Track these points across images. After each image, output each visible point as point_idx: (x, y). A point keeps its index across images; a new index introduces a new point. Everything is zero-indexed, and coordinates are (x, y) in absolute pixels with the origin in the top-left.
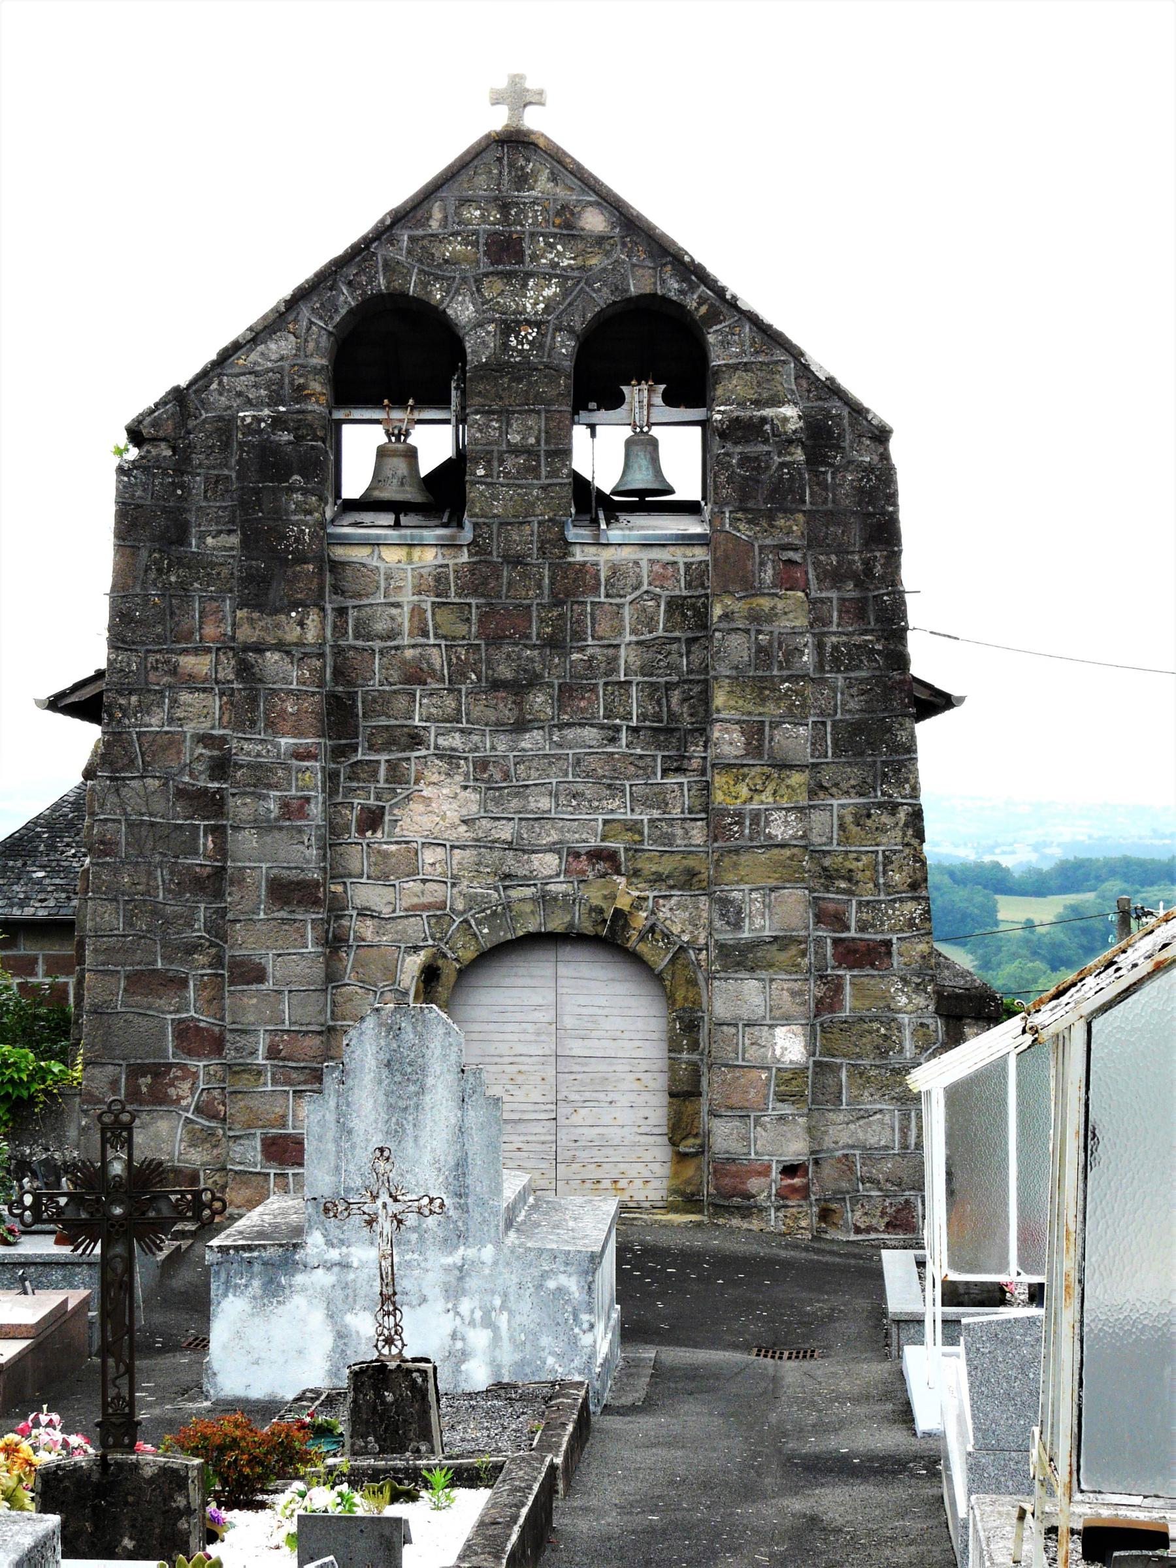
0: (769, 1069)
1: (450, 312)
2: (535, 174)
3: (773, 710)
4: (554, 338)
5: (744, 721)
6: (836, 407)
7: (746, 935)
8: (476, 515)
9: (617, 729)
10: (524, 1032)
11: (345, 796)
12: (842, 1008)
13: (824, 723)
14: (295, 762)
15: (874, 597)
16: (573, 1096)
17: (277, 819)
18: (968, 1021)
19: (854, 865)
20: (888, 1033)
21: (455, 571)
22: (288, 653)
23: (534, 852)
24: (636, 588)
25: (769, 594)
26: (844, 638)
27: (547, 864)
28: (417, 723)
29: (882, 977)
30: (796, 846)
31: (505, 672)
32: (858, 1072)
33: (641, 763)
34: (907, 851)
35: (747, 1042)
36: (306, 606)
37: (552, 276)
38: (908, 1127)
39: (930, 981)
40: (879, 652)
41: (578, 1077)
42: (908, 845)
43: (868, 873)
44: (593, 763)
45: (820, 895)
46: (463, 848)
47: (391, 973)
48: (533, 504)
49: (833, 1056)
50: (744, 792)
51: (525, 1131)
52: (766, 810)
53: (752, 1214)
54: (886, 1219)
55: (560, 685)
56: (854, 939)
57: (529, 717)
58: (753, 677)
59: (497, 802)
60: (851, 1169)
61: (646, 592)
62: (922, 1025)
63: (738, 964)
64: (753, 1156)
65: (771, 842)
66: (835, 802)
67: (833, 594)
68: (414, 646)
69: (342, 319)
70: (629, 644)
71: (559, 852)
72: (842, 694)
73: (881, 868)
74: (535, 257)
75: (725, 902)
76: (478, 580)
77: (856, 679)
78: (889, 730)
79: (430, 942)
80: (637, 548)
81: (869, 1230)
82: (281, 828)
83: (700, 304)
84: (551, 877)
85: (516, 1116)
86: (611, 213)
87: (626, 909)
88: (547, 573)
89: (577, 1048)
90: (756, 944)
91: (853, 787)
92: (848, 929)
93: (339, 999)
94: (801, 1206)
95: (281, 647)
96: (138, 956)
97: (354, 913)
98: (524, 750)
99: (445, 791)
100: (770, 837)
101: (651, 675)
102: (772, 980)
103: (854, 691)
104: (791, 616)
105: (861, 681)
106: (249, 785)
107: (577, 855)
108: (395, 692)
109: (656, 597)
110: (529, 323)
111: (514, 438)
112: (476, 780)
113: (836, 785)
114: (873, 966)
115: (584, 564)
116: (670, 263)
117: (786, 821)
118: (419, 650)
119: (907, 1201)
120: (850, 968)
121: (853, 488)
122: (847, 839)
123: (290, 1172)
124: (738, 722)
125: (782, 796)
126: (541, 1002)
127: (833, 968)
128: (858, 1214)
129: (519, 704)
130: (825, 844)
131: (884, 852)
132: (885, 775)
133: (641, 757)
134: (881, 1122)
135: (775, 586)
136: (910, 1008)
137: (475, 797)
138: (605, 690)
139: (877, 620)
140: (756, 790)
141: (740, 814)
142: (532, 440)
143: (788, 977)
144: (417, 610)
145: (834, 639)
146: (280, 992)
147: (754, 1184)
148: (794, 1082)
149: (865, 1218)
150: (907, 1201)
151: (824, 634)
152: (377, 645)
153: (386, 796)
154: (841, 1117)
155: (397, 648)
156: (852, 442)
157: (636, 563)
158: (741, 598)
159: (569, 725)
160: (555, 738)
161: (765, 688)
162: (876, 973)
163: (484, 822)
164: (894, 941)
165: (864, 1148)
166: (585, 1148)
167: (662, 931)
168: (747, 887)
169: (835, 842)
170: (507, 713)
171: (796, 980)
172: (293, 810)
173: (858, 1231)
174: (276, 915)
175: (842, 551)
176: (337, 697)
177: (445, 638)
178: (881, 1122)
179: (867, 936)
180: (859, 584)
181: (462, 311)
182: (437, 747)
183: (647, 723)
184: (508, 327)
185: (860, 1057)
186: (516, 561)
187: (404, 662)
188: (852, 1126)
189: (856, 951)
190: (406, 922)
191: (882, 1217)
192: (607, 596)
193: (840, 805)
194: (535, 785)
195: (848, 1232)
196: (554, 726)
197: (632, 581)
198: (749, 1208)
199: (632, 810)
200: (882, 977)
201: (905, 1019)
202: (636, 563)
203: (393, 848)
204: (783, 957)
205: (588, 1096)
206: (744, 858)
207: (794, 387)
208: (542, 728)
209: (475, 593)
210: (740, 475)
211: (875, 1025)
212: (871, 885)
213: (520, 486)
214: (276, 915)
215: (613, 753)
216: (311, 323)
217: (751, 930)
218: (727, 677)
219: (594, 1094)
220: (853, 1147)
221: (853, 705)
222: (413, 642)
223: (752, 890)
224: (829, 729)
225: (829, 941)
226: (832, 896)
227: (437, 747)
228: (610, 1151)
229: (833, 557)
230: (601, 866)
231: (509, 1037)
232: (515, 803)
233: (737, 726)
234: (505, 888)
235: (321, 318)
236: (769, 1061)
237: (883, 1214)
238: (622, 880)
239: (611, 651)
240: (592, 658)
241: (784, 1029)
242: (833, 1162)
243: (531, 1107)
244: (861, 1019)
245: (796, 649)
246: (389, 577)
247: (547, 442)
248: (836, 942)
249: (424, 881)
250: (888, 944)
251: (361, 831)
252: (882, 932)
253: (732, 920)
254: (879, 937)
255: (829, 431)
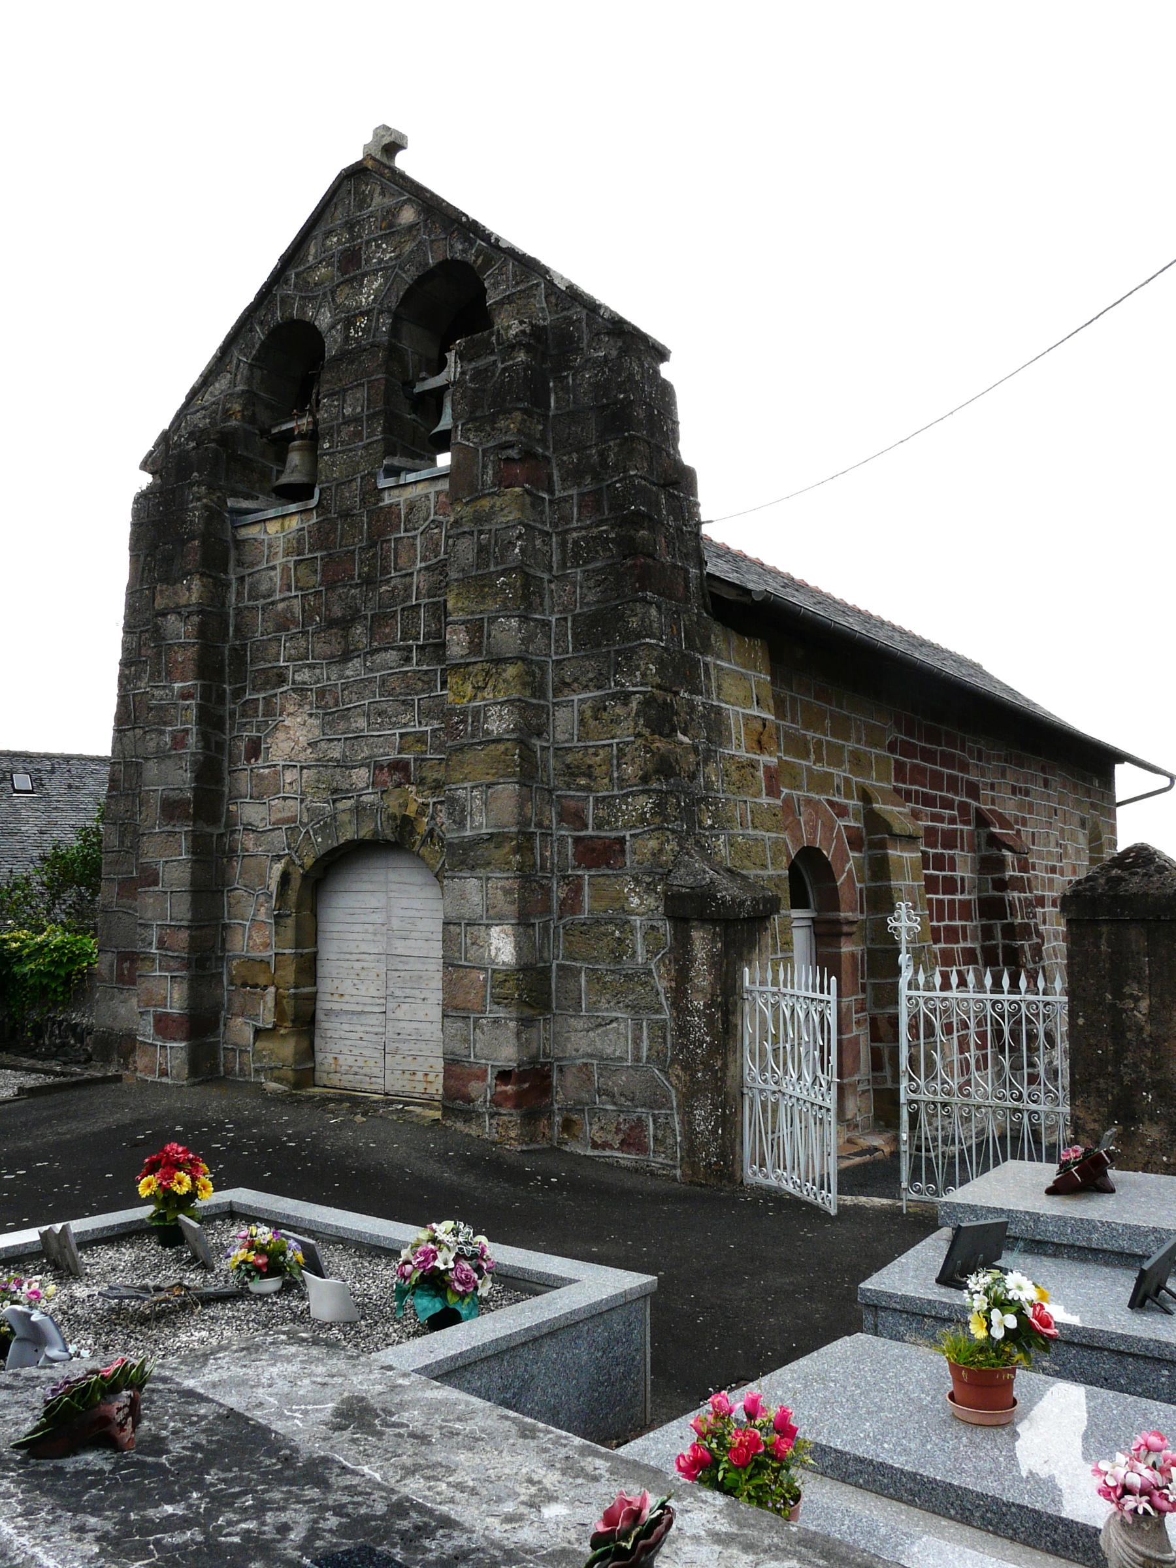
0: (486, 969)
1: (316, 323)
2: (372, 193)
3: (492, 606)
4: (378, 320)
5: (468, 621)
6: (578, 313)
7: (468, 833)
8: (322, 482)
9: (409, 649)
10: (367, 932)
11: (239, 731)
12: (581, 910)
13: (565, 619)
14: (181, 702)
15: (608, 486)
16: (398, 993)
17: (170, 750)
18: (695, 924)
19: (590, 761)
20: (623, 936)
21: (309, 532)
22: (179, 613)
23: (353, 767)
24: (426, 520)
25: (489, 494)
26: (584, 532)
27: (361, 776)
28: (282, 664)
29: (616, 876)
30: (508, 740)
31: (337, 612)
32: (595, 977)
33: (425, 678)
34: (639, 741)
35: (469, 941)
36: (191, 574)
37: (377, 271)
38: (640, 1038)
39: (661, 880)
40: (613, 540)
41: (402, 974)
42: (638, 735)
43: (604, 767)
44: (394, 683)
45: (563, 793)
46: (308, 767)
47: (263, 878)
48: (358, 463)
49: (575, 960)
50: (469, 690)
51: (365, 1022)
52: (486, 706)
53: (472, 1119)
54: (621, 1136)
55: (372, 616)
56: (592, 837)
57: (352, 648)
58: (475, 576)
59: (331, 724)
60: (590, 1078)
61: (433, 521)
62: (653, 927)
63: (463, 863)
64: (472, 1059)
65: (489, 738)
66: (576, 698)
67: (574, 492)
68: (283, 600)
69: (258, 351)
70: (419, 571)
71: (368, 766)
72: (581, 587)
73: (615, 762)
74: (368, 260)
75: (452, 801)
76: (322, 537)
77: (594, 571)
78: (621, 617)
79: (287, 851)
80: (427, 483)
81: (605, 1145)
82: (170, 757)
83: (477, 257)
84: (363, 789)
85: (359, 1008)
86: (419, 205)
87: (412, 815)
88: (365, 519)
89: (401, 947)
90: (477, 841)
91: (591, 680)
92: (586, 827)
93: (233, 901)
94: (511, 1115)
95: (176, 610)
96: (125, 868)
97: (241, 828)
98: (348, 677)
99: (299, 720)
100: (487, 732)
101: (434, 596)
102: (488, 879)
103: (592, 583)
104: (505, 512)
105: (597, 571)
106: (155, 724)
107: (381, 768)
108: (269, 640)
109: (439, 525)
110: (362, 314)
111: (348, 411)
112: (317, 707)
113: (576, 680)
114: (608, 865)
115: (391, 505)
116: (457, 229)
117: (501, 716)
118: (286, 603)
119: (639, 1119)
120: (588, 868)
121: (590, 384)
122: (587, 733)
123: (168, 1045)
124: (464, 623)
125: (499, 691)
126: (377, 905)
127: (574, 868)
128: (595, 1127)
129: (345, 637)
130: (566, 741)
131: (618, 744)
132: (619, 664)
133: (426, 672)
134: (617, 1030)
135: (494, 485)
136: (642, 909)
137: (316, 722)
138: (402, 615)
139: (610, 510)
140: (479, 687)
141: (464, 712)
142: (359, 409)
143: (505, 875)
144: (285, 569)
145: (575, 535)
146: (166, 893)
147: (474, 1088)
148: (507, 984)
149: (601, 1133)
150: (639, 1119)
151: (567, 531)
152: (262, 602)
153: (262, 728)
154: (579, 1024)
155: (273, 603)
156: (589, 342)
157: (427, 496)
158: (467, 503)
159: (378, 650)
160: (368, 664)
161: (484, 586)
162: (610, 872)
163: (323, 743)
164: (628, 838)
165: (601, 1058)
166: (405, 1041)
167: (439, 836)
168: (467, 785)
169: (576, 738)
170: (337, 649)
171: (507, 878)
172: (179, 740)
173: (595, 1146)
174: (166, 828)
175: (581, 448)
176: (235, 650)
177: (302, 589)
178: (617, 1030)
179: (603, 834)
180: (597, 478)
181: (324, 319)
182: (294, 682)
183: (431, 641)
184: (349, 323)
185: (597, 962)
186: (346, 515)
187: (278, 614)
188: (591, 1034)
189: (593, 850)
190: (273, 834)
191: (616, 1133)
192: (406, 531)
193: (579, 700)
194: (355, 707)
195: (586, 1146)
196: (367, 653)
197: (423, 514)
198: (469, 1112)
199: (420, 723)
200: (616, 876)
201: (637, 920)
202: (427, 496)
203: (267, 771)
204: (498, 854)
205: (408, 992)
206: (468, 756)
207: (545, 305)
208: (359, 656)
209: (320, 549)
210: (471, 389)
211: (611, 928)
212: (606, 780)
213: (350, 450)
214: (166, 828)
215: (408, 672)
216: (240, 361)
217: (472, 828)
218: (456, 580)
219: (413, 991)
220: (591, 1056)
221: (590, 598)
222: (282, 596)
223: (473, 788)
224: (569, 624)
225: (570, 840)
226: (572, 793)
227: (294, 682)
228: (422, 1045)
229: (575, 456)
230: (397, 776)
231: (355, 936)
232: (342, 725)
233: (463, 627)
234: (334, 801)
235: (245, 355)
236: (486, 961)
237: (618, 1130)
238: (413, 788)
239: (408, 579)
240: (395, 587)
241: (498, 929)
242: (574, 1070)
243: (369, 1000)
244: (597, 922)
245: (510, 542)
246: (270, 546)
247: (368, 408)
248: (577, 840)
249: (285, 798)
250: (621, 841)
251: (248, 760)
252: (616, 829)
253: (457, 818)
254: (614, 834)
255: (571, 335)
